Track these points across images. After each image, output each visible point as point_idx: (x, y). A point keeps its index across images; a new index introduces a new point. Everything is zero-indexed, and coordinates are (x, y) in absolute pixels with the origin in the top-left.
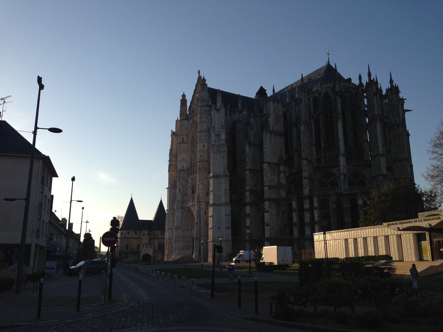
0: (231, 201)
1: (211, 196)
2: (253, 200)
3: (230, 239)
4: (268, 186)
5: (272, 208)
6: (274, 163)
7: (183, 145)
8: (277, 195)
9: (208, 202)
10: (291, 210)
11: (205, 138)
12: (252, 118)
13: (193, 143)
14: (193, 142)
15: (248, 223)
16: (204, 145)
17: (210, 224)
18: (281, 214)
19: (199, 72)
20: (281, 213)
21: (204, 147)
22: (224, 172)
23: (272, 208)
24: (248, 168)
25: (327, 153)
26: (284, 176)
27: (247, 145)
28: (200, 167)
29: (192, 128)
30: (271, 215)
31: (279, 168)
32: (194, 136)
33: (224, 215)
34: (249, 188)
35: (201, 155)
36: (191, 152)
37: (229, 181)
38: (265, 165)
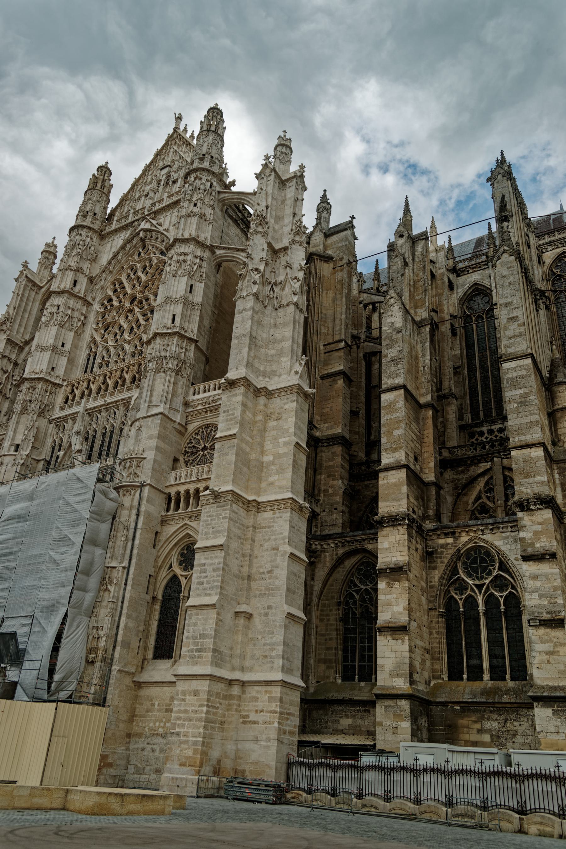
7: (72, 302)
9: (178, 493)
11: (200, 266)
12: (401, 236)
13: (115, 303)
14: (114, 298)
16: (192, 286)
19: (179, 118)
21: (191, 292)
24: (399, 381)
27: (392, 305)
28: (163, 354)
29: (120, 258)
32: (125, 281)
34: (403, 458)
35: (174, 316)
36: (96, 330)
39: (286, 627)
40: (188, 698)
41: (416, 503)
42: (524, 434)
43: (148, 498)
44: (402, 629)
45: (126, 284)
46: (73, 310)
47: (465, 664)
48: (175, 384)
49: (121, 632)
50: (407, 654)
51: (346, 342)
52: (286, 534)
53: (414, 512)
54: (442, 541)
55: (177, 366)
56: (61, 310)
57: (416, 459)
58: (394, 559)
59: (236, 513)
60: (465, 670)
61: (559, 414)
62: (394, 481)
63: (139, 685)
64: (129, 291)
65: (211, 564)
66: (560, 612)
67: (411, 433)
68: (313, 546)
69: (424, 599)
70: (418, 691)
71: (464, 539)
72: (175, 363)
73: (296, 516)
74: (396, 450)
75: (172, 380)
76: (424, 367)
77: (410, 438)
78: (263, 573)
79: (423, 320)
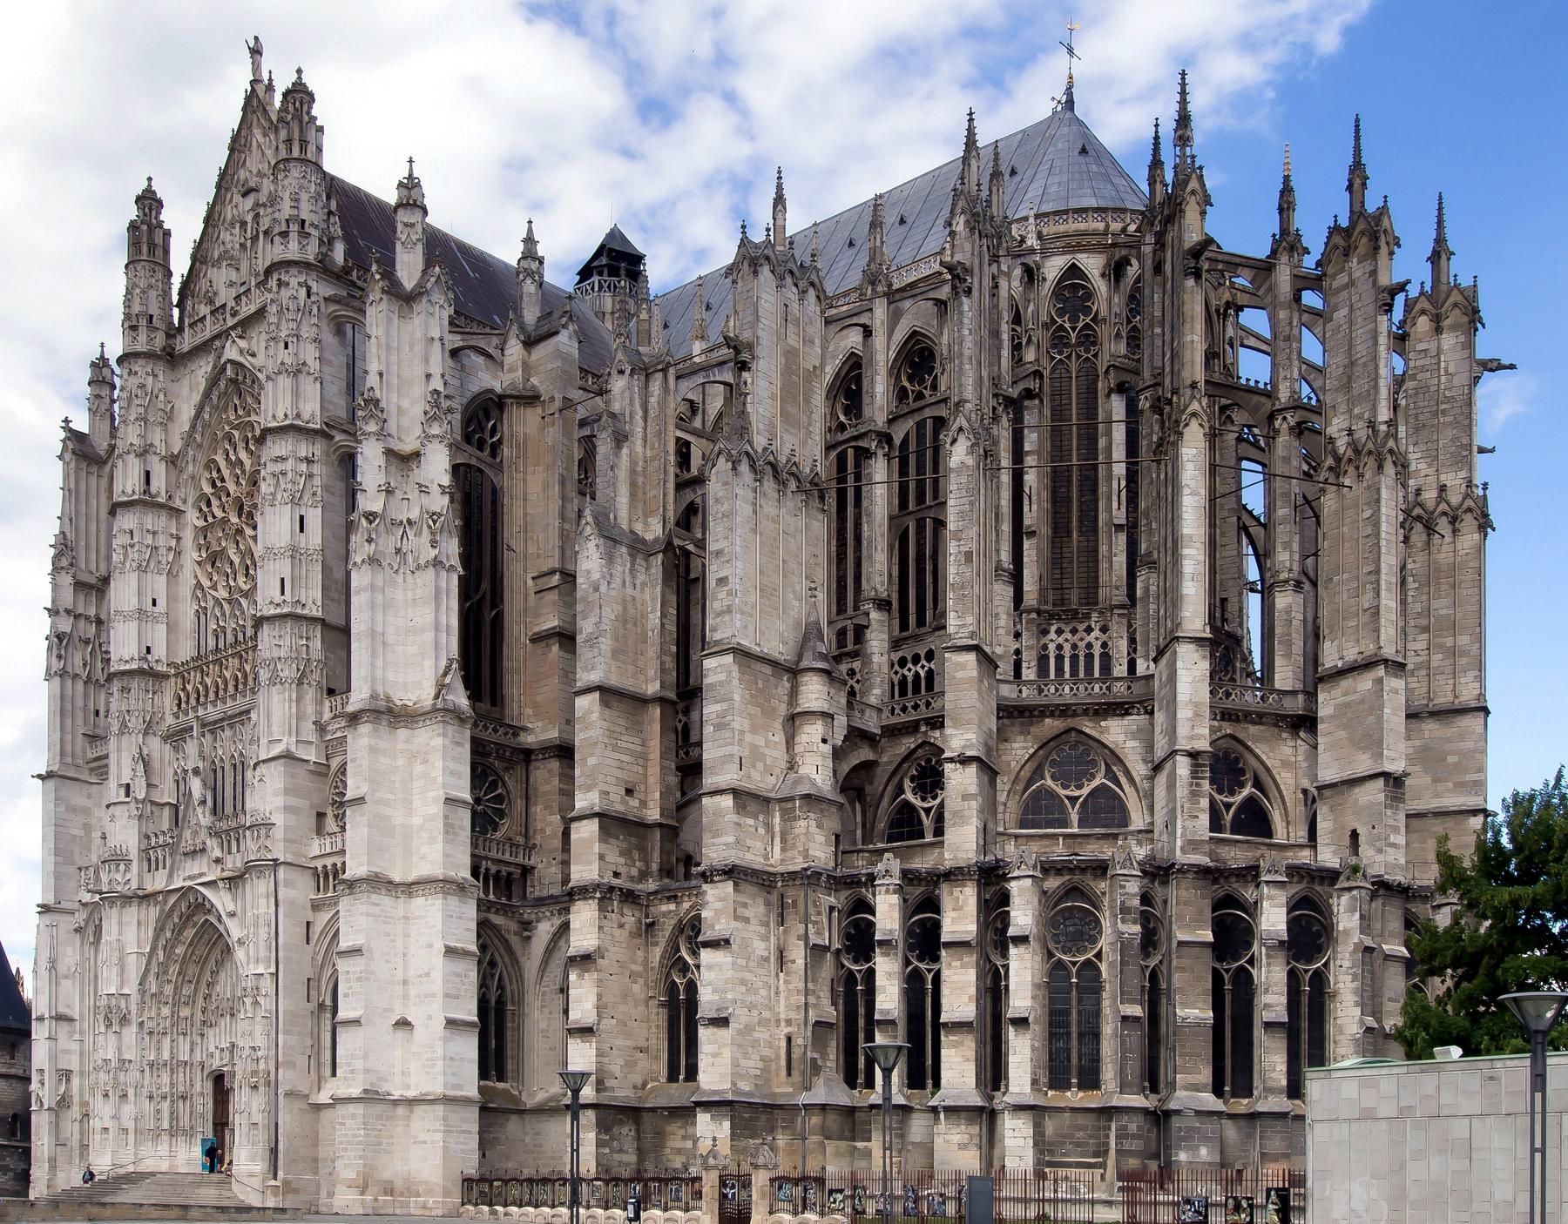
0: (475, 872)
1: (358, 828)
2: (616, 875)
3: (472, 1091)
4: (736, 792)
5: (747, 920)
6: (774, 663)
8: (777, 848)
10: (861, 940)
15: (583, 1006)
17: (346, 995)
18: (800, 962)
20: (798, 955)
22: (441, 688)
23: (747, 920)
24: (594, 677)
25: (1053, 635)
26: (824, 741)
30: (742, 962)
31: (794, 693)
33: (439, 947)
34: (597, 801)
37: (468, 746)
38: (716, 670)
39: (445, 1040)
40: (347, 1122)
41: (622, 861)
43: (285, 880)
44: (586, 1031)
45: (226, 473)
46: (154, 533)
48: (298, 701)
49: (280, 1052)
50: (594, 1059)
51: (561, 572)
52: (440, 927)
54: (664, 908)
55: (298, 670)
56: (136, 540)
57: (629, 792)
58: (585, 943)
61: (797, 723)
62: (585, 835)
63: (318, 1108)
64: (232, 487)
65: (355, 972)
66: (727, 1008)
69: (637, 988)
71: (686, 905)
72: (294, 666)
73: (453, 901)
74: (589, 789)
75: (294, 697)
76: (653, 631)
77: (616, 764)
78: (421, 976)
79: (656, 540)
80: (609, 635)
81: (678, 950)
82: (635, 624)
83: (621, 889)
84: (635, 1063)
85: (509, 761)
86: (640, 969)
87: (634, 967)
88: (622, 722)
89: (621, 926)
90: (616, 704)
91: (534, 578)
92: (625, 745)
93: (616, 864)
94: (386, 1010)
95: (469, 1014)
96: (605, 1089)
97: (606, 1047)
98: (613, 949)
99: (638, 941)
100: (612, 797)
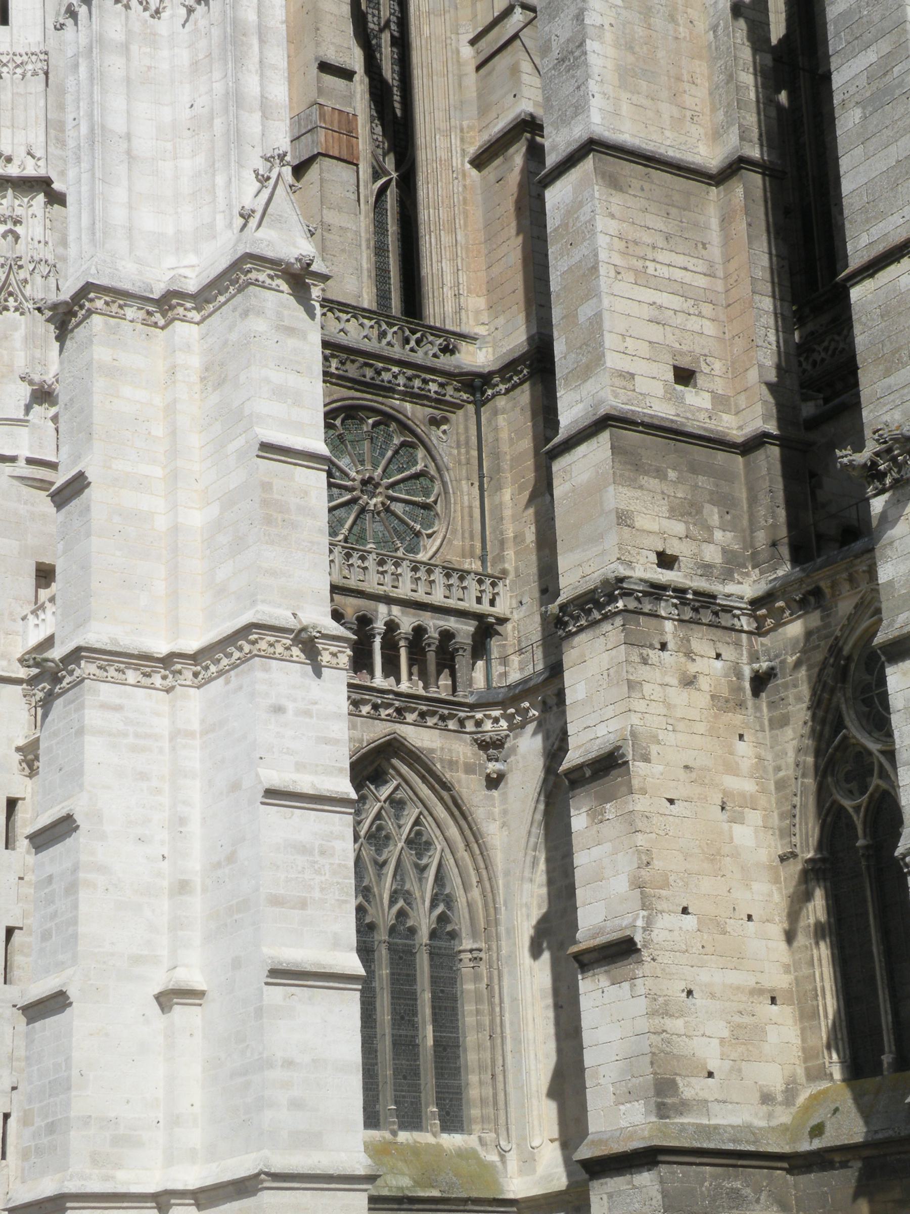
41: (679, 528)
42: (883, 216)
47: (886, 1020)
53: (666, 561)
57: (684, 376)
58: (601, 730)
59: (118, 708)
60: (888, 1039)
67: (649, 295)
68: (488, 726)
70: (703, 1130)
77: (646, 312)
80: (609, 36)
81: (839, 725)
82: (672, 19)
83: (680, 592)
84: (757, 1033)
85: (439, 402)
86: (748, 786)
87: (733, 783)
88: (653, 221)
89: (689, 682)
90: (636, 183)
91: (473, 42)
92: (664, 271)
93: (662, 534)
94: (137, 960)
95: (336, 944)
96: (683, 1107)
97: (676, 989)
98: (670, 738)
99: (737, 719)
100: (642, 385)
